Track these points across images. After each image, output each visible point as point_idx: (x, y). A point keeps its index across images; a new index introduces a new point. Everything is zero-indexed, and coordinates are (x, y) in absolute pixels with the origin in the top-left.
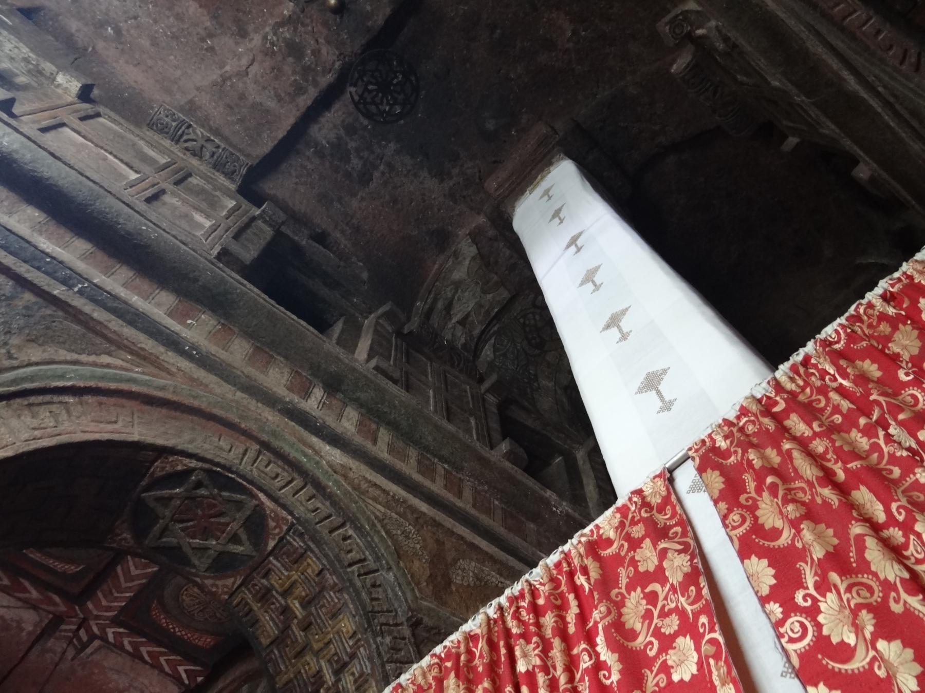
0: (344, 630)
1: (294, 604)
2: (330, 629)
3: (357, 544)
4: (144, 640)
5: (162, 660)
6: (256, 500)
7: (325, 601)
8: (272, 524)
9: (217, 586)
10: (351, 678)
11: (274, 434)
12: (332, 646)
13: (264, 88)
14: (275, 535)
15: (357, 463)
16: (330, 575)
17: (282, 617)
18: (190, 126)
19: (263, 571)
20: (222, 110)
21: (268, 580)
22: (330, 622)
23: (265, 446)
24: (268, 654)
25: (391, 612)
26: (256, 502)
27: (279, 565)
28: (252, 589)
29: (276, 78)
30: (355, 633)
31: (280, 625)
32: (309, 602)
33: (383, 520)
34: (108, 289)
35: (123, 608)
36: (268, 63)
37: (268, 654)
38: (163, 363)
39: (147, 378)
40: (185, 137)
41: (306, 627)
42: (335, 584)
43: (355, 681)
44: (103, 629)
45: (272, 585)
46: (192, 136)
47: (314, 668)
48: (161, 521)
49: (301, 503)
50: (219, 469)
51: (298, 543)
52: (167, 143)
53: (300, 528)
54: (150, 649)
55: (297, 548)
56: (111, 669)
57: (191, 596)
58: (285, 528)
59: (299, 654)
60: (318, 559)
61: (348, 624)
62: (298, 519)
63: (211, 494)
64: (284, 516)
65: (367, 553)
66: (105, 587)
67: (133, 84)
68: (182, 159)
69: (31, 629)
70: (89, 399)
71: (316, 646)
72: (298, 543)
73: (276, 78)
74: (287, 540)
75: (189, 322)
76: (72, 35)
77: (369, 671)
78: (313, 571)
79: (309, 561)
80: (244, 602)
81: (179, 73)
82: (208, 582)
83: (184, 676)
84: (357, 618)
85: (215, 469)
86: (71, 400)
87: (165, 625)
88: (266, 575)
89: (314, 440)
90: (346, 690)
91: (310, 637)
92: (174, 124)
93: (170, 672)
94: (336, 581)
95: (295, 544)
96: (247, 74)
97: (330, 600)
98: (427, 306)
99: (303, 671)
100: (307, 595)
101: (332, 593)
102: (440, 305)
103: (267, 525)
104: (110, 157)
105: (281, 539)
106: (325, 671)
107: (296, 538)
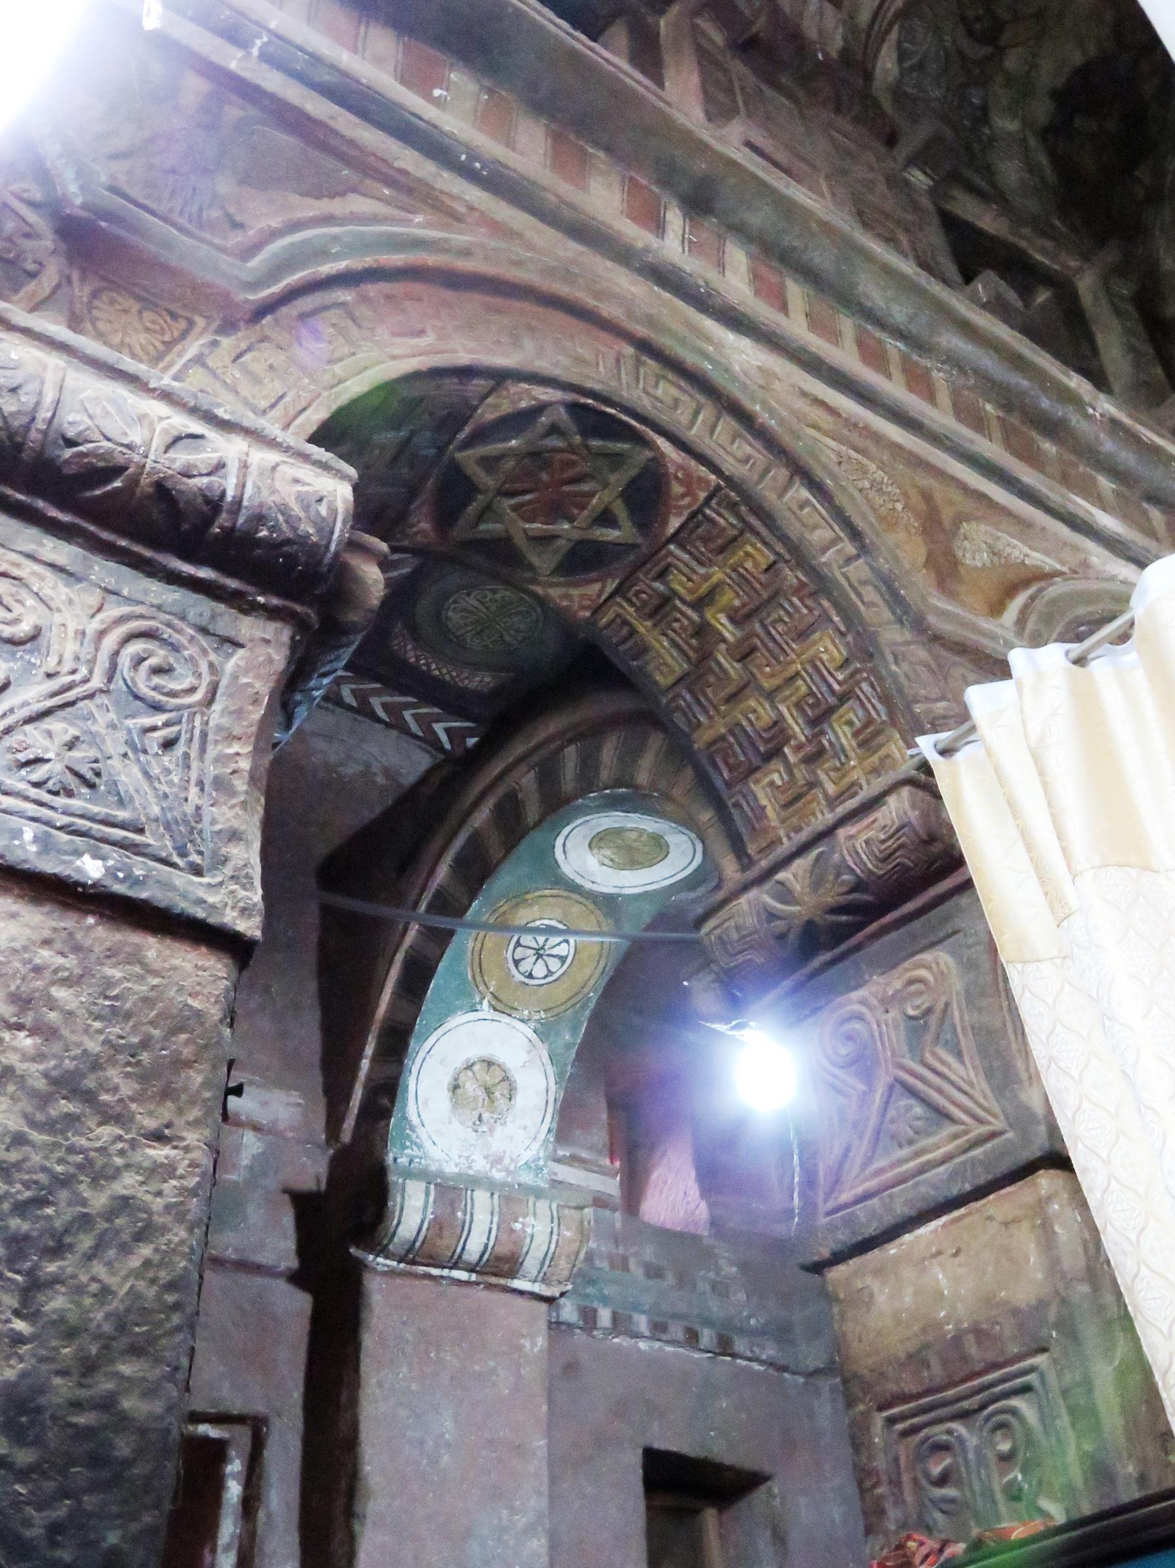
0: (825, 657)
1: (717, 620)
2: (794, 657)
4: (378, 686)
5: (407, 715)
6: (651, 449)
7: (782, 613)
8: (677, 489)
9: (567, 596)
10: (846, 729)
11: (651, 321)
12: (800, 682)
14: (680, 507)
16: (791, 570)
17: (694, 642)
19: (657, 569)
21: (666, 584)
22: (794, 646)
23: (645, 347)
24: (674, 698)
26: (648, 454)
27: (686, 557)
28: (634, 599)
30: (847, 660)
31: (691, 654)
32: (748, 616)
37: (674, 698)
38: (445, 198)
41: (745, 655)
42: (803, 585)
43: (856, 734)
45: (675, 593)
47: (765, 713)
48: (479, 497)
50: (590, 401)
51: (725, 520)
53: (733, 494)
55: (725, 529)
56: (316, 734)
57: (464, 610)
58: (702, 495)
59: (733, 698)
60: (765, 543)
61: (831, 647)
62: (729, 480)
63: (570, 445)
64: (702, 474)
65: (836, 527)
70: (372, 289)
71: (767, 684)
72: (725, 520)
74: (705, 516)
77: (884, 718)
78: (756, 564)
79: (749, 549)
80: (619, 621)
82: (555, 593)
83: (444, 738)
84: (850, 638)
85: (583, 400)
86: (345, 295)
87: (413, 660)
88: (662, 575)
90: (838, 746)
91: (755, 671)
93: (420, 734)
94: (804, 579)
95: (721, 521)
97: (791, 610)
99: (744, 723)
100: (744, 605)
101: (795, 600)
103: (668, 492)
105: (693, 515)
106: (790, 721)
107: (723, 511)
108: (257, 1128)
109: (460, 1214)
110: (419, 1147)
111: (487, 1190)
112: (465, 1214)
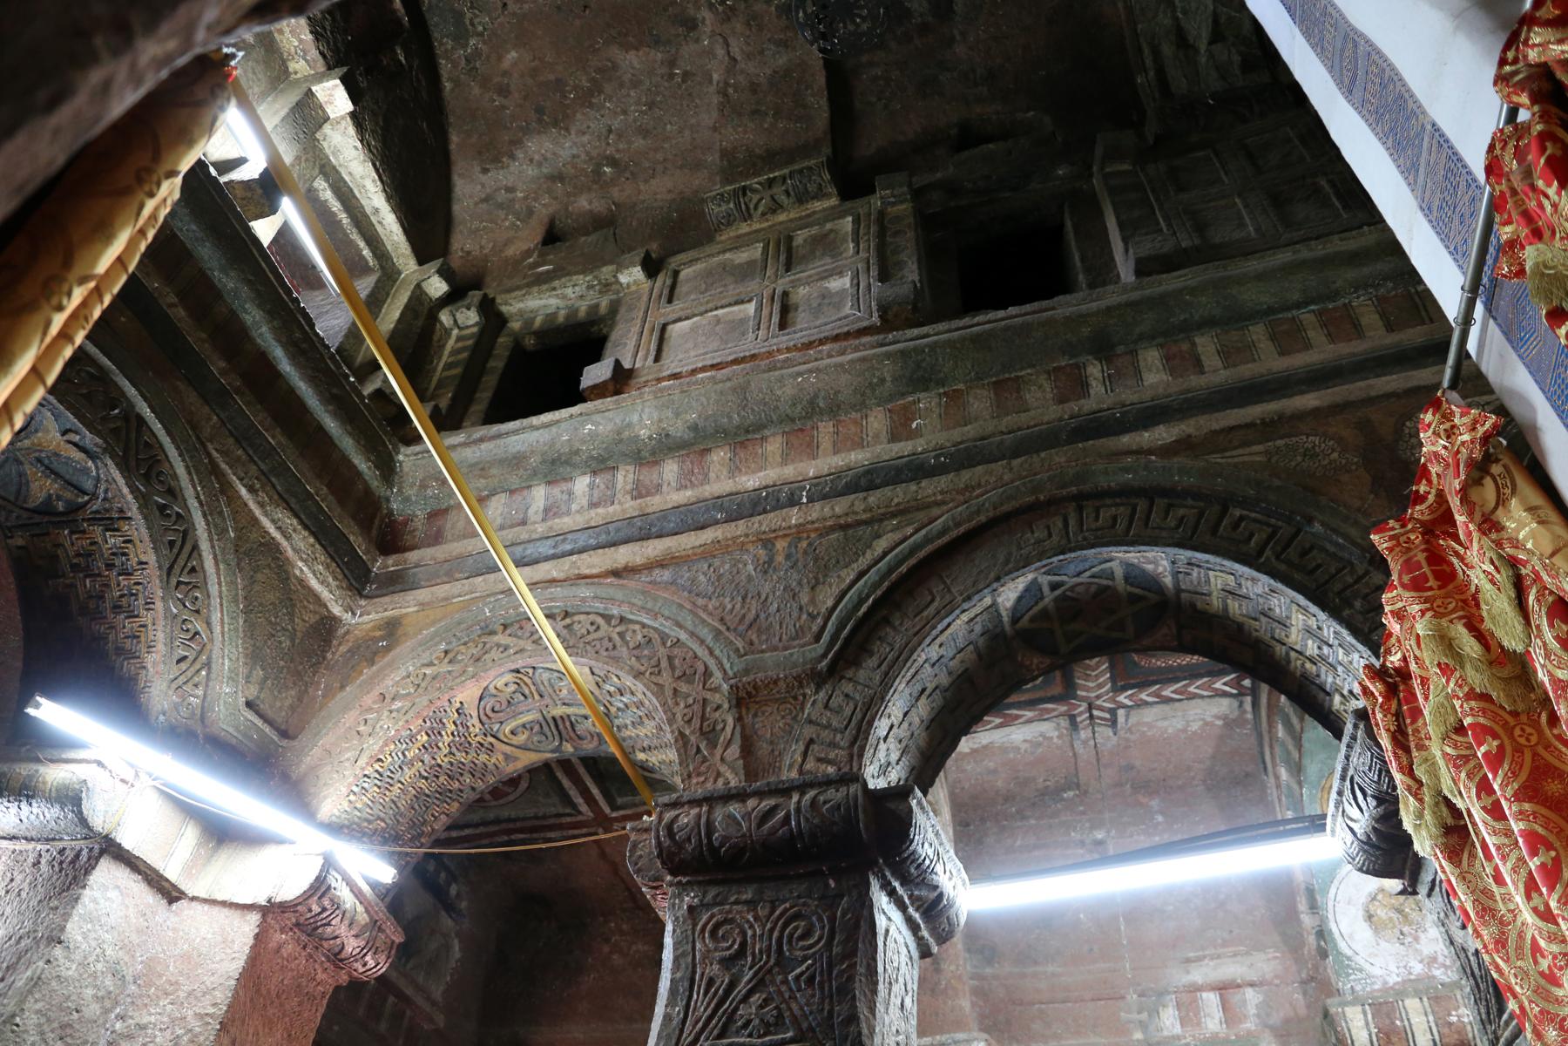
3: (1255, 520)
5: (1192, 689)
13: (762, 52)
15: (1192, 421)
18: (744, 189)
20: (751, 125)
23: (1080, 499)
25: (1344, 568)
29: (760, 28)
33: (1269, 460)
34: (826, 471)
35: (1111, 677)
36: (738, 26)
39: (923, 532)
40: (752, 206)
44: (1113, 700)
46: (755, 198)
49: (1160, 528)
52: (744, 228)
54: (1172, 689)
66: (1078, 674)
67: (669, 197)
68: (770, 227)
69: (1056, 733)
73: (760, 28)
75: (914, 425)
76: (591, 211)
81: (687, 133)
83: (1227, 689)
89: (1126, 440)
92: (732, 205)
96: (735, 60)
98: (1152, 74)
102: (1167, 50)
104: (720, 312)
108: (1252, 985)
109: (1398, 1022)
110: (1361, 970)
111: (1413, 997)
112: (1402, 1021)
